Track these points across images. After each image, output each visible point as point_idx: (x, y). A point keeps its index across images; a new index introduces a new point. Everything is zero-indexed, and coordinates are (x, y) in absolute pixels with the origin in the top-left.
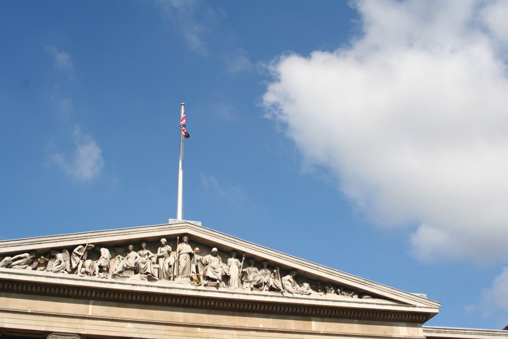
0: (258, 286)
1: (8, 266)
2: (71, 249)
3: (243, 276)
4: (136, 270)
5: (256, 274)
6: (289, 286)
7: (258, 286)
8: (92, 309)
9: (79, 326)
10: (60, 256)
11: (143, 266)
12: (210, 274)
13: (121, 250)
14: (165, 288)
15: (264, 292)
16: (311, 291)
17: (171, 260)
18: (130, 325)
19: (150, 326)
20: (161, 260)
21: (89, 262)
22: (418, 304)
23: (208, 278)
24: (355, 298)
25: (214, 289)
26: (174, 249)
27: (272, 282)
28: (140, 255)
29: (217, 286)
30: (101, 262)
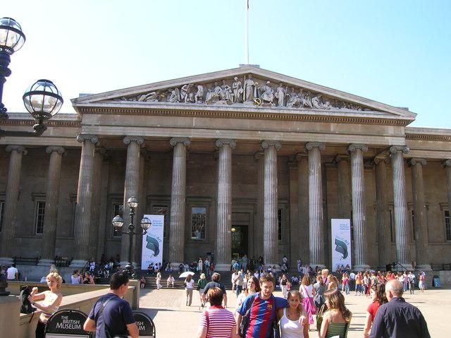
0: (296, 105)
1: (145, 100)
2: (180, 88)
3: (286, 99)
4: (220, 99)
5: (295, 99)
6: (316, 104)
7: (296, 105)
8: (195, 121)
9: (188, 133)
10: (173, 92)
11: (223, 95)
12: (265, 98)
13: (210, 86)
14: (237, 108)
15: (299, 109)
16: (330, 107)
17: (241, 90)
18: (218, 131)
19: (230, 131)
20: (235, 91)
21: (191, 95)
22: (402, 114)
23: (265, 101)
24: (360, 111)
25: (268, 107)
26: (243, 83)
27: (304, 102)
28: (223, 89)
29: (270, 105)
30: (199, 94)
